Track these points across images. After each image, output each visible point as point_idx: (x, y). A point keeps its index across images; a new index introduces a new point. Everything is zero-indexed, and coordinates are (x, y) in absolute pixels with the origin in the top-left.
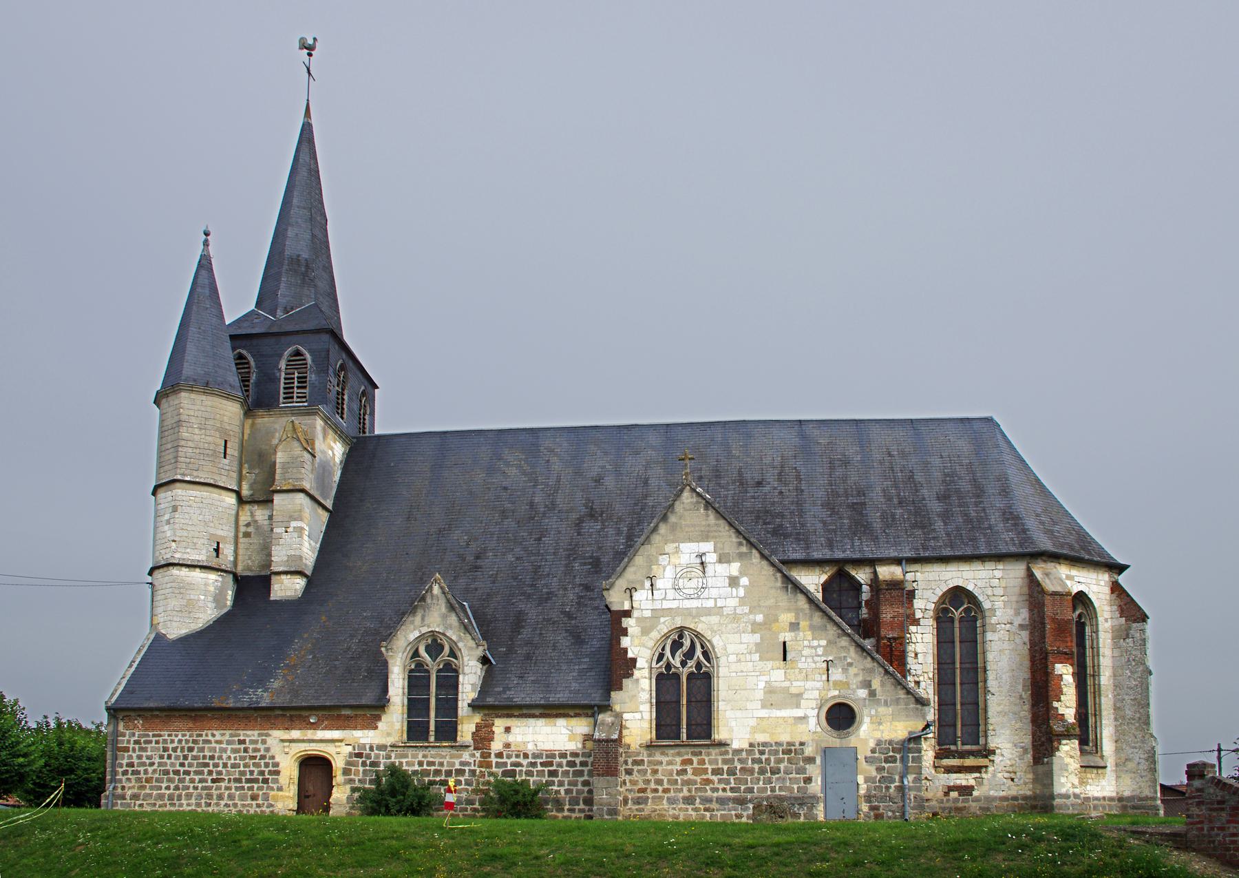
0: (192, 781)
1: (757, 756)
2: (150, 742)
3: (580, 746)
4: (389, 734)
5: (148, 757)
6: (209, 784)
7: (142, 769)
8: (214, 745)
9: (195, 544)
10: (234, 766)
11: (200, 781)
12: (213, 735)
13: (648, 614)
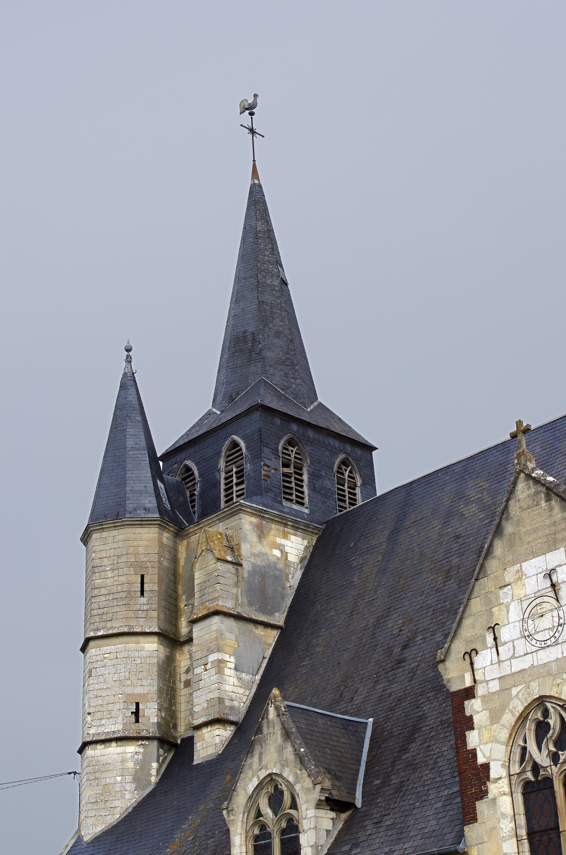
9: (110, 711)
13: (495, 686)
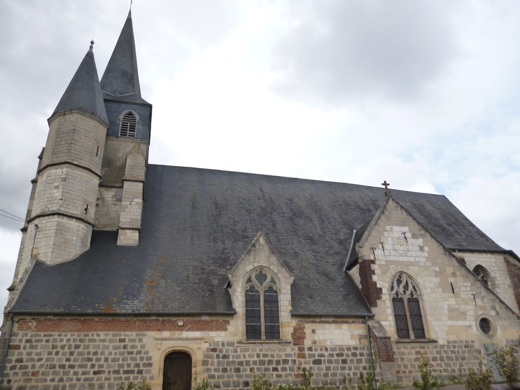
0: (76, 373)
1: (452, 349)
2: (41, 341)
3: (358, 342)
4: (235, 334)
5: (37, 354)
6: (91, 375)
7: (30, 364)
8: (98, 343)
9: (74, 203)
10: (114, 360)
11: (83, 373)
12: (98, 335)
13: (383, 263)
